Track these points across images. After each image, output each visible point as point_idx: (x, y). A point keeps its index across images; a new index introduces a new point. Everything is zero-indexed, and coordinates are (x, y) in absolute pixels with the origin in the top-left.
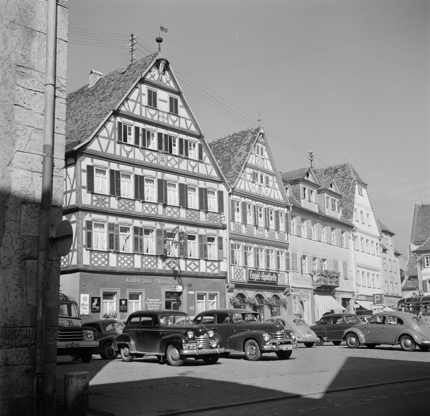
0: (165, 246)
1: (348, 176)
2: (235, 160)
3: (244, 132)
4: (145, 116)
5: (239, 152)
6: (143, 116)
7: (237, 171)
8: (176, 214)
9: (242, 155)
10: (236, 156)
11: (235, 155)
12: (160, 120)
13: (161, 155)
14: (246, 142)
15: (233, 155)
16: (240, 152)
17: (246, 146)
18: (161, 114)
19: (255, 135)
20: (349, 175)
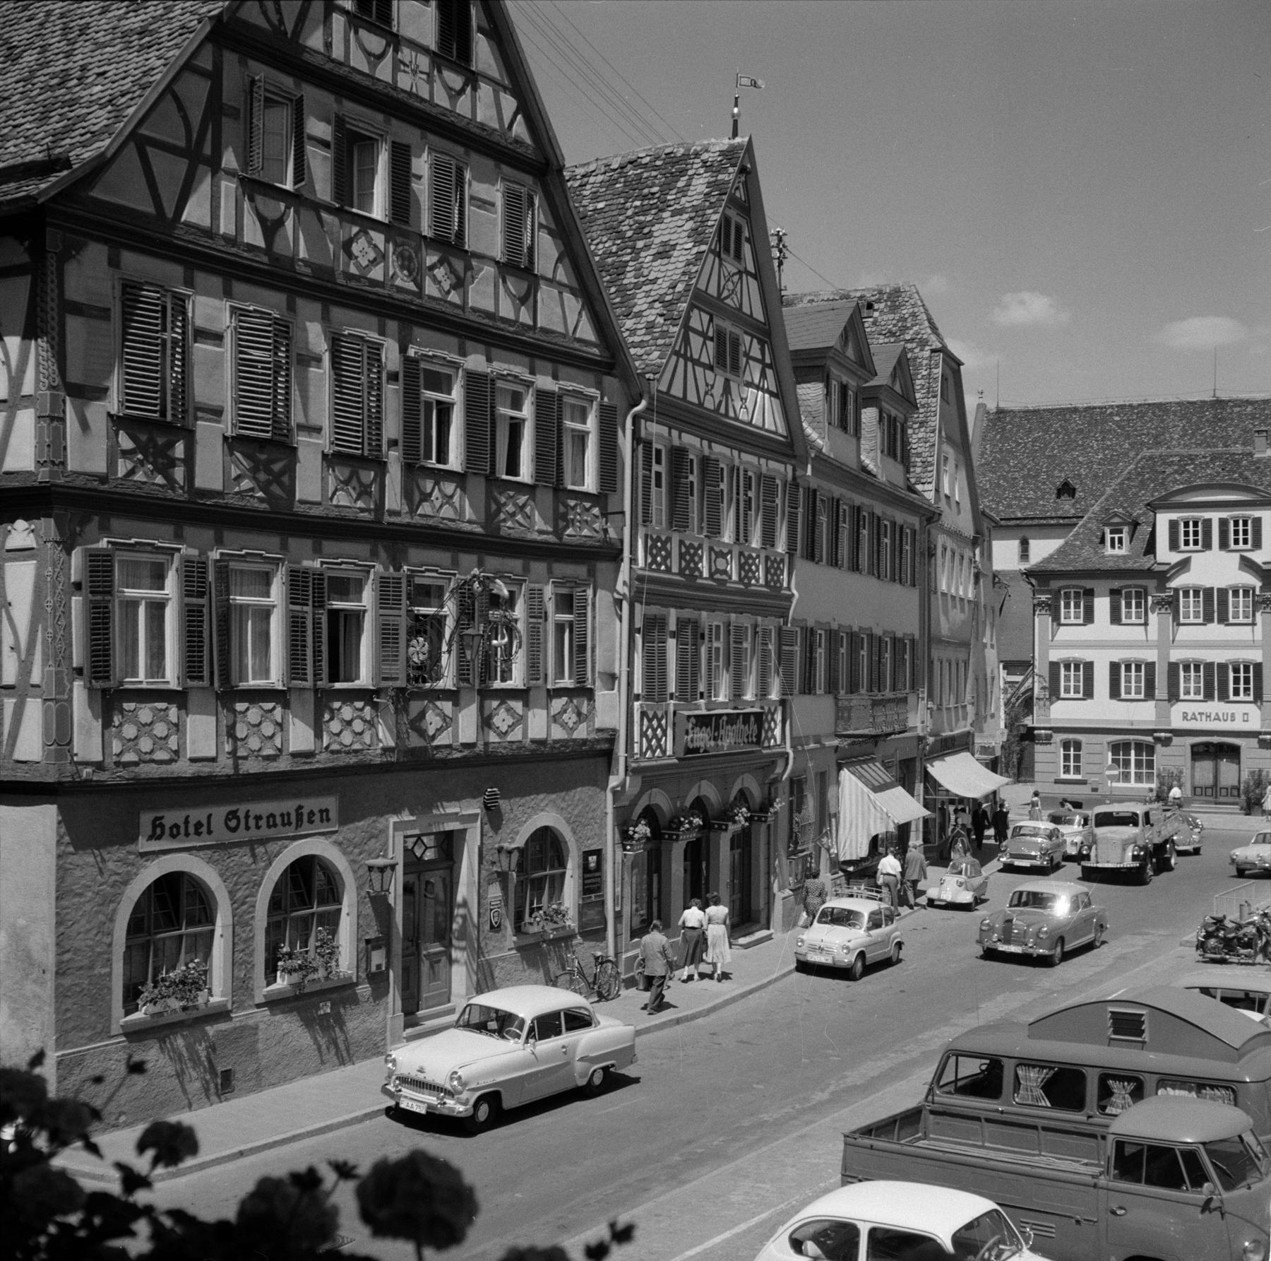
0: (411, 649)
2: (646, 272)
3: (671, 159)
4: (342, 59)
5: (657, 241)
6: (334, 56)
7: (661, 320)
8: (452, 505)
9: (676, 253)
10: (646, 257)
11: (641, 250)
12: (400, 85)
13: (403, 245)
14: (683, 200)
15: (634, 248)
16: (665, 238)
17: (686, 216)
18: (406, 54)
19: (720, 177)
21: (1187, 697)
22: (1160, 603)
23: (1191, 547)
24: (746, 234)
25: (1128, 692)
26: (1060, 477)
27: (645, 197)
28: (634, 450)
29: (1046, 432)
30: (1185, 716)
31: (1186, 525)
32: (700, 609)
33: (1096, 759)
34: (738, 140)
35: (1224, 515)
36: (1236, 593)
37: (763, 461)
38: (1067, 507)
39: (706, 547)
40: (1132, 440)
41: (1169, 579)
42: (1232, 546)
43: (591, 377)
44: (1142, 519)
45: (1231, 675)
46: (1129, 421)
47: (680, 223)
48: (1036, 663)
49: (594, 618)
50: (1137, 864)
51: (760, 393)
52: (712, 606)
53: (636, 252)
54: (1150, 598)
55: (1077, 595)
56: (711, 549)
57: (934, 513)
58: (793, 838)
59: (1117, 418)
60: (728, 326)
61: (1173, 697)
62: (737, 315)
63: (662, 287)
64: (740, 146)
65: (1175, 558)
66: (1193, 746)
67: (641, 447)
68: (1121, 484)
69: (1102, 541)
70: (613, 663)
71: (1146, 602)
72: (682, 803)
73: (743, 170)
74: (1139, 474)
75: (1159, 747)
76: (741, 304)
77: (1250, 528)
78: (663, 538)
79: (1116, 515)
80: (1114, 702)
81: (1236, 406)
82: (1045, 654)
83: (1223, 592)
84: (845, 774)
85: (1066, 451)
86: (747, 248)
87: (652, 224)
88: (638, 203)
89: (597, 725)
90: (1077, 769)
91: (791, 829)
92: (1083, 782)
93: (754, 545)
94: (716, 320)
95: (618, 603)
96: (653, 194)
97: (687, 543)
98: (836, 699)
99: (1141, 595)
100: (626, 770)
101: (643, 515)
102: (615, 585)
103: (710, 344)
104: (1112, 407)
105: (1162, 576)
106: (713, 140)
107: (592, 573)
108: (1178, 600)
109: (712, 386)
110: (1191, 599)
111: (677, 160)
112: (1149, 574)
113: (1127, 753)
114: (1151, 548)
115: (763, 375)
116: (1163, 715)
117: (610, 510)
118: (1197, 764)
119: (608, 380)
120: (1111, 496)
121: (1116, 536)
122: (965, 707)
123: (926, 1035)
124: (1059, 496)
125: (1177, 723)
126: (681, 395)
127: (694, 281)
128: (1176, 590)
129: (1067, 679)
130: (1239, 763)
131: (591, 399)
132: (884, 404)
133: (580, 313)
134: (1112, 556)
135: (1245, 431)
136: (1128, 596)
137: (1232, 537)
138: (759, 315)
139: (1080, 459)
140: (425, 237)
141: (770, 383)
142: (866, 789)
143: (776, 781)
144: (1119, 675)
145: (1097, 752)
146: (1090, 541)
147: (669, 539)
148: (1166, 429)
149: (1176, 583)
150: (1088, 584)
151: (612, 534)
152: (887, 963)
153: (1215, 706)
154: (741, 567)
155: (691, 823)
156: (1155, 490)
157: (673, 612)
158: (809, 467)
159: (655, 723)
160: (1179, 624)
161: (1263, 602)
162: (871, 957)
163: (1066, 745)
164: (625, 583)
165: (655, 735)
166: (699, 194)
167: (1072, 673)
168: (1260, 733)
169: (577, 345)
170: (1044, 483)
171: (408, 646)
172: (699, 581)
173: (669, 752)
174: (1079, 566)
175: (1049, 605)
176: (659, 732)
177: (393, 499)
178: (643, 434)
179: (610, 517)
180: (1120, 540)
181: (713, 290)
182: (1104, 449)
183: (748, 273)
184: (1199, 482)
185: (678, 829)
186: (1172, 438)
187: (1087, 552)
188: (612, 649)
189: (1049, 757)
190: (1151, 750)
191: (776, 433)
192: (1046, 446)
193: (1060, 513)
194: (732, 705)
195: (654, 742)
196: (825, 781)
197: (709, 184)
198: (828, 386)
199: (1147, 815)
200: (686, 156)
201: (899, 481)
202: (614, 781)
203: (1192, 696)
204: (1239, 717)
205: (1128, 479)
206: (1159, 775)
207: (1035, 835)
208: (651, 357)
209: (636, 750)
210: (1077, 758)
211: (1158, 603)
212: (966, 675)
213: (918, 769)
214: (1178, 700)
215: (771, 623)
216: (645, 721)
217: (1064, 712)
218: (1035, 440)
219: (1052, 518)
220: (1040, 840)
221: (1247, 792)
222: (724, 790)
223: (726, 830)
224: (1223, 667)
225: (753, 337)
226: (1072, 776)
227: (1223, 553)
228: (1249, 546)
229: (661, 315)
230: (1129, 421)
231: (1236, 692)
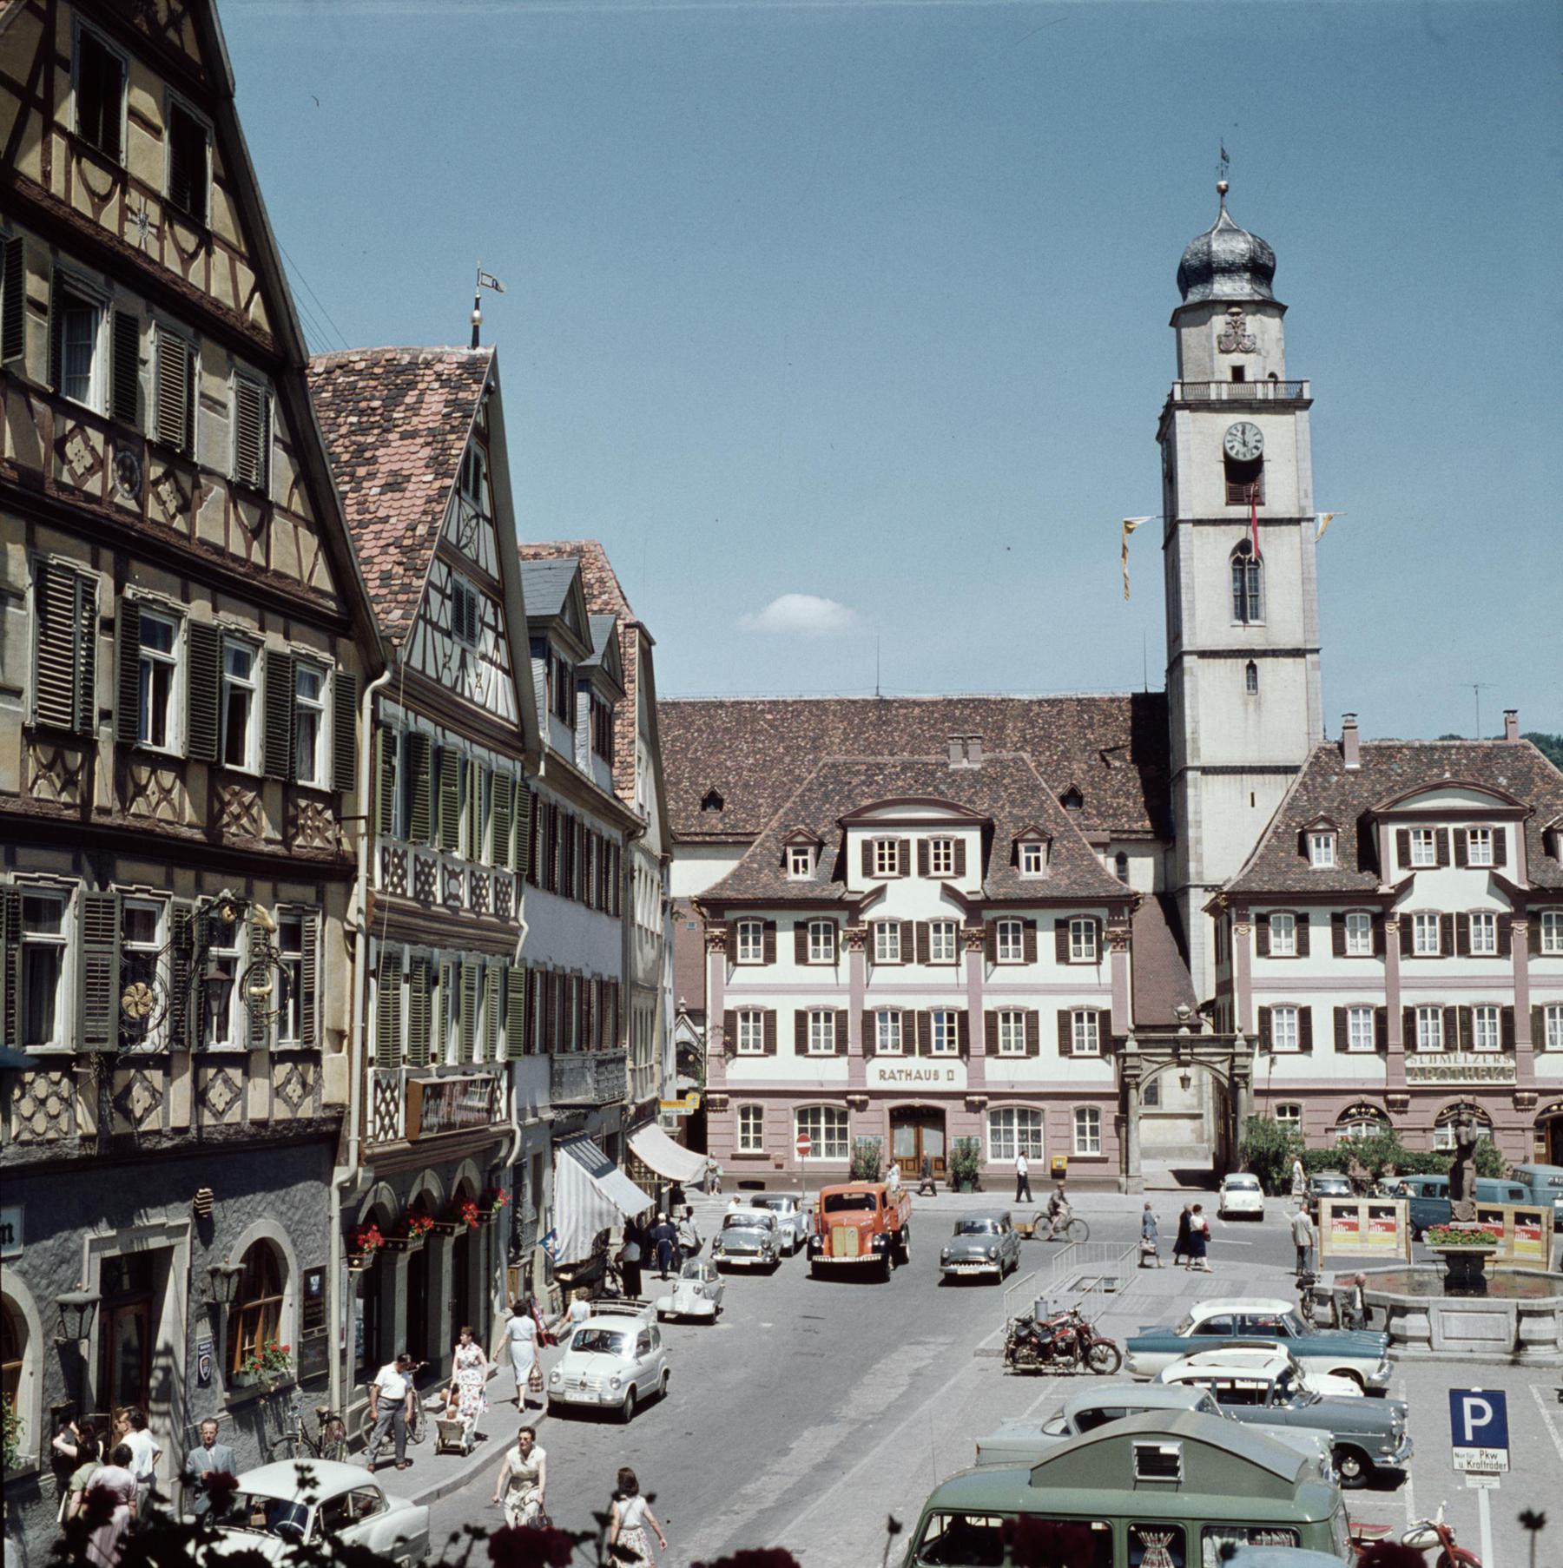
0: (127, 999)
2: (372, 508)
3: (393, 368)
4: (62, 195)
6: (53, 190)
7: (400, 570)
8: (170, 802)
9: (411, 487)
10: (372, 489)
11: (364, 478)
12: (127, 238)
13: (124, 449)
14: (415, 420)
15: (352, 475)
16: (395, 467)
17: (420, 441)
18: (134, 199)
19: (461, 395)
20: (605, 597)
21: (884, 1052)
22: (853, 940)
23: (887, 873)
24: (484, 469)
27: (362, 413)
28: (373, 736)
30: (882, 1075)
31: (881, 846)
33: (782, 1128)
34: (479, 351)
35: (924, 835)
36: (937, 928)
37: (493, 755)
39: (439, 864)
40: (787, 743)
41: (862, 911)
42: (933, 873)
44: (828, 839)
45: (934, 1025)
46: (783, 720)
47: (413, 449)
50: (878, 1257)
54: (841, 934)
55: (756, 929)
56: (444, 867)
57: (638, 825)
58: (515, 1243)
59: (769, 717)
61: (869, 1051)
63: (397, 526)
64: (484, 359)
65: (869, 885)
66: (892, 1111)
67: (380, 732)
68: (802, 796)
69: (784, 863)
74: (821, 785)
75: (853, 1112)
79: (800, 833)
81: (901, 707)
82: (718, 1000)
83: (923, 926)
85: (711, 754)
86: (484, 485)
88: (354, 419)
90: (758, 1142)
91: (514, 1229)
92: (765, 1158)
94: (455, 575)
96: (374, 409)
97: (422, 858)
98: (552, 1060)
103: (448, 603)
104: (763, 702)
105: (854, 909)
106: (447, 348)
108: (872, 936)
111: (403, 370)
112: (839, 904)
113: (816, 1120)
114: (840, 873)
115: (497, 647)
116: (857, 1074)
118: (897, 1132)
119: (344, 644)
120: (791, 809)
121: (800, 858)
123: (749, 1489)
124: (704, 808)
125: (874, 1083)
126: (420, 667)
127: (440, 523)
128: (871, 924)
130: (943, 1130)
131: (324, 667)
132: (594, 689)
134: (796, 882)
135: (912, 736)
136: (816, 929)
137: (876, 862)
138: (494, 572)
140: (150, 442)
141: (501, 657)
142: (589, 1176)
144: (805, 1026)
145: (781, 1119)
146: (770, 864)
148: (824, 731)
150: (770, 915)
152: (656, 1397)
153: (916, 1062)
156: (840, 803)
157: (407, 947)
158: (542, 765)
159: (388, 1095)
160: (874, 965)
161: (969, 939)
162: (642, 1390)
163: (745, 1113)
165: (388, 1111)
169: (312, 596)
171: (122, 995)
174: (760, 893)
177: (103, 794)
178: (381, 716)
180: (805, 863)
183: (485, 518)
186: (832, 743)
187: (766, 876)
188: (341, 998)
189: (723, 1128)
190: (844, 1117)
191: (507, 720)
192: (688, 746)
195: (387, 1121)
196: (539, 1164)
197: (447, 403)
198: (549, 664)
199: (884, 1195)
200: (413, 365)
201: (606, 784)
204: (943, 1076)
205: (810, 790)
206: (854, 1148)
207: (749, 1225)
208: (391, 616)
210: (758, 1128)
211: (851, 939)
214: (874, 1056)
215: (494, 964)
217: (746, 1071)
218: (675, 739)
219: (697, 834)
221: (955, 1163)
223: (451, 1234)
224: (924, 1016)
225: (487, 597)
226: (752, 1150)
227: (923, 880)
228: (951, 873)
229: (399, 564)
230: (783, 720)
231: (939, 1047)
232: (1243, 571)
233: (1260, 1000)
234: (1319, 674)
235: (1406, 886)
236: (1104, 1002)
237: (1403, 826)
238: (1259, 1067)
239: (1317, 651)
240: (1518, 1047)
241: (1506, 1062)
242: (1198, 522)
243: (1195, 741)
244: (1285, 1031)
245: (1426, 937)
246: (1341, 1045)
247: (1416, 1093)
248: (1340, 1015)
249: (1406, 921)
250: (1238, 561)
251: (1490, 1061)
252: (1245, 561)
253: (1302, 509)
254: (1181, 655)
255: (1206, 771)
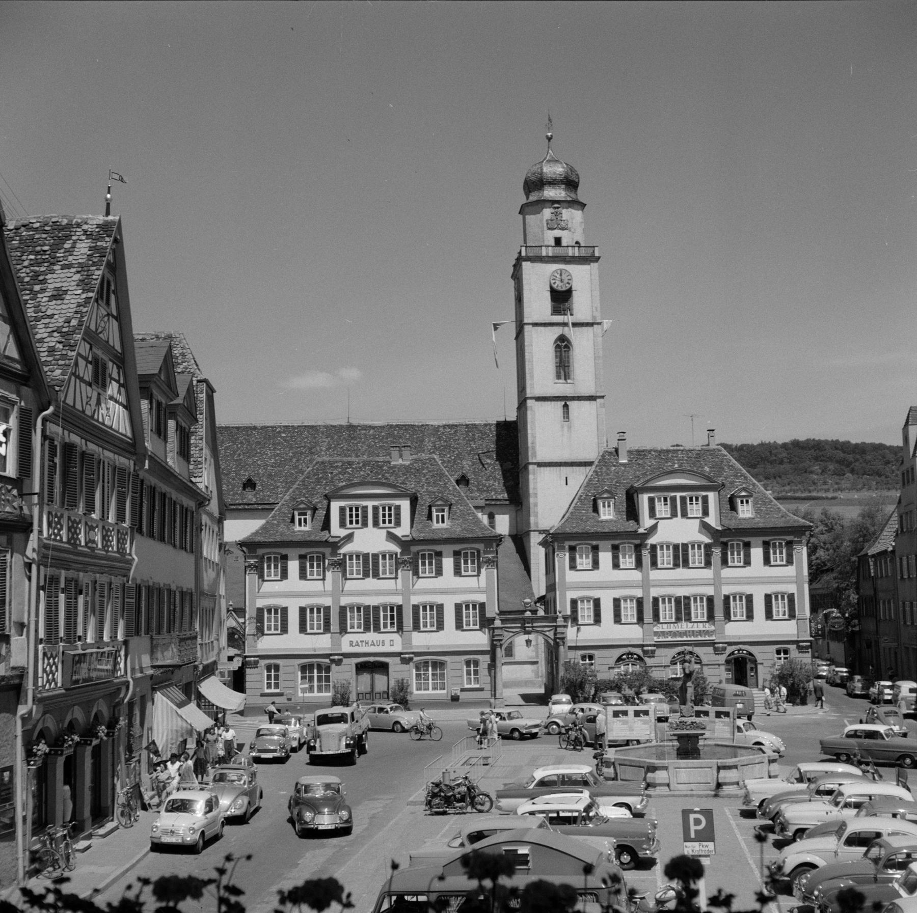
1: (182, 367)
2: (43, 309)
7: (60, 346)
9: (67, 297)
10: (43, 298)
14: (70, 258)
15: (31, 290)
16: (58, 285)
17: (73, 270)
19: (99, 244)
20: (184, 364)
22: (334, 564)
23: (354, 525)
24: (113, 288)
25: (312, 628)
26: (244, 476)
27: (37, 253)
28: (42, 445)
29: (234, 443)
32: (79, 570)
34: (110, 218)
36: (384, 557)
38: (250, 497)
41: (339, 548)
42: (381, 525)
43: (13, 386)
44: (319, 506)
48: (247, 609)
49: (11, 577)
51: (117, 405)
52: (85, 567)
53: (34, 295)
54: (327, 561)
57: (205, 498)
59: (284, 435)
60: (99, 353)
62: (106, 346)
63: (59, 321)
65: (343, 533)
68: (303, 481)
69: (293, 521)
70: (23, 614)
71: (324, 563)
72: (63, 726)
73: (116, 241)
76: (108, 338)
77: (393, 512)
78: (59, 514)
79: (302, 502)
80: (302, 635)
81: (363, 429)
83: (375, 556)
84: (158, 696)
86: (113, 297)
87: (44, 273)
88: (32, 257)
89: (11, 665)
93: (110, 521)
94: (94, 350)
95: (28, 566)
96: (45, 251)
99: (321, 558)
100: (34, 700)
101: (47, 497)
102: (25, 551)
103: (90, 366)
105: (335, 546)
107: (10, 542)
109: (91, 398)
110: (354, 561)
111: (63, 228)
112: (326, 544)
114: (326, 525)
115: (119, 392)
117: (24, 492)
119: (25, 390)
121: (302, 517)
122: (212, 642)
124: (244, 488)
126: (72, 404)
127: (85, 319)
128: (345, 555)
129: (269, 620)
131: (13, 404)
132: (179, 419)
133: (8, 337)
134: (299, 531)
135: (369, 446)
137: (348, 519)
138: (118, 348)
139: (259, 462)
141: (122, 399)
143: (119, 704)
146: (285, 521)
147: (62, 516)
148: (317, 443)
149: (346, 549)
150: (284, 551)
151: (26, 511)
154: (104, 538)
155: (72, 740)
156: (326, 485)
160: (346, 579)
161: (403, 563)
164: (34, 550)
166: (82, 254)
167: (273, 615)
168: (402, 653)
169: (6, 361)
170: (233, 479)
172: (79, 548)
173: (59, 685)
175: (256, 567)
176: (54, 668)
179: (25, 497)
180: (305, 520)
181: (93, 327)
182: (275, 457)
183: (113, 316)
184: (355, 481)
185: (62, 745)
186: (321, 450)
187: (282, 528)
189: (258, 678)
193: (245, 501)
194: (111, 644)
197: (90, 248)
198: (151, 403)
201: (185, 475)
202: (22, 710)
203: (356, 630)
205: (308, 477)
208: (54, 374)
209: (40, 684)
211: (332, 564)
212: (213, 617)
213: (193, 689)
216: (46, 661)
218: (227, 448)
219: (240, 504)
220: (276, 738)
222: (87, 713)
225: (114, 363)
227: (375, 529)
228: (392, 525)
229: (60, 342)
230: (291, 437)
231: (385, 626)
232: (561, 352)
233: (571, 595)
234: (604, 410)
235: (654, 528)
236: (482, 598)
237: (652, 495)
238: (571, 633)
239: (603, 397)
240: (716, 619)
241: (709, 627)
242: (535, 325)
243: (534, 448)
244: (585, 612)
245: (665, 557)
246: (617, 619)
247: (659, 645)
248: (617, 602)
249: (653, 548)
250: (558, 347)
251: (701, 627)
252: (563, 345)
253: (594, 317)
254: (525, 399)
255: (540, 465)
